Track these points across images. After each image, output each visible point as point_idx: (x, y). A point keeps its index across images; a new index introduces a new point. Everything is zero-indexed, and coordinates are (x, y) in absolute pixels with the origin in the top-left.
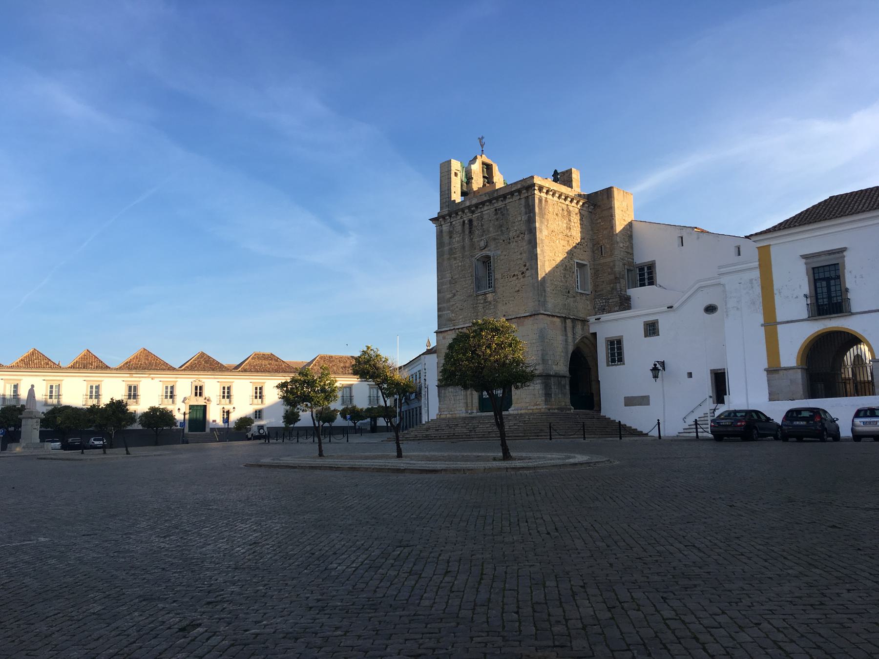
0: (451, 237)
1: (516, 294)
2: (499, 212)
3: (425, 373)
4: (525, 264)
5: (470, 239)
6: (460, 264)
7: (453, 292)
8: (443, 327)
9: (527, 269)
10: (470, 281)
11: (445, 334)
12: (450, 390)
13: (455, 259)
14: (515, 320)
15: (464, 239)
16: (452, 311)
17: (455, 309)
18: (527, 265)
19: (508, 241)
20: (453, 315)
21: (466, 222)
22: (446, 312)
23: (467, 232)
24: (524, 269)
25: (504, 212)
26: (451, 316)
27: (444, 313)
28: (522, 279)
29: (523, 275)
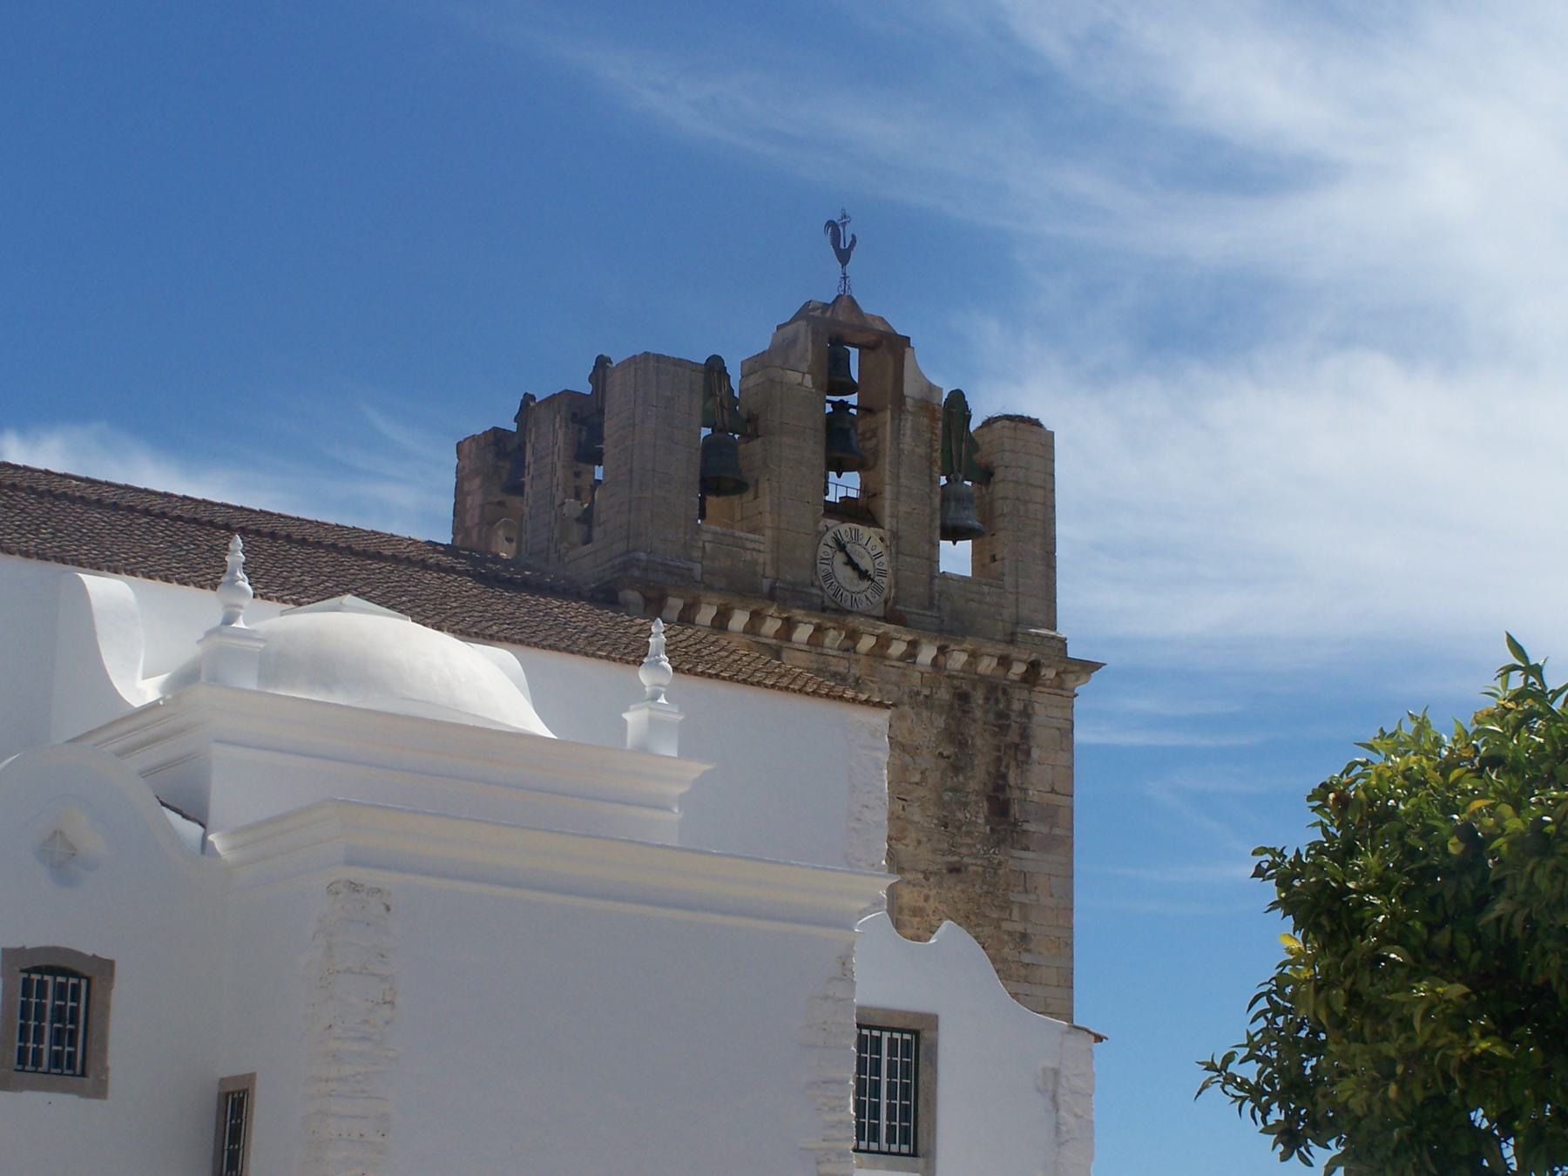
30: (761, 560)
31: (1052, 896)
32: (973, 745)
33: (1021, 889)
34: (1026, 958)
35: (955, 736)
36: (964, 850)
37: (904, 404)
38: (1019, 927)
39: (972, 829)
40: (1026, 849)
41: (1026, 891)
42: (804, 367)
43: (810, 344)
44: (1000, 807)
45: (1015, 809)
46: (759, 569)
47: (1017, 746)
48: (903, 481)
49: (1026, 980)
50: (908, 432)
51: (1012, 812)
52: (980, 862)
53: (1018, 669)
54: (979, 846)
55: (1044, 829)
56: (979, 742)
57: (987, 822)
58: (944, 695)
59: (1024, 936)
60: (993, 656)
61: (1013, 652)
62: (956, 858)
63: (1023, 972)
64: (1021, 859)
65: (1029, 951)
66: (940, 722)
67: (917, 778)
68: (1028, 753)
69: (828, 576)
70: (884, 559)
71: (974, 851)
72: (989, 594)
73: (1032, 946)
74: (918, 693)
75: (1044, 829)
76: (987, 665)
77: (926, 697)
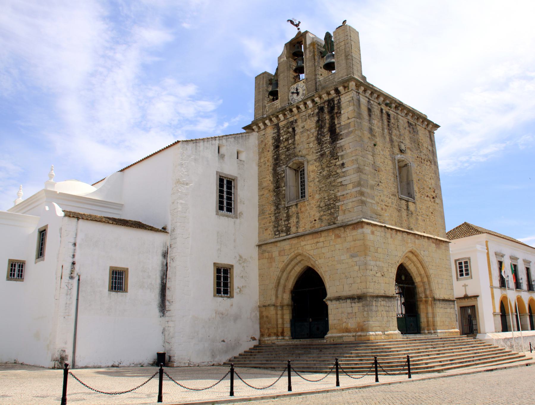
0: (370, 115)
2: (411, 126)
5: (389, 133)
7: (377, 180)
8: (368, 217)
10: (393, 179)
11: (374, 229)
12: (383, 303)
15: (383, 130)
18: (436, 192)
19: (420, 159)
21: (384, 111)
23: (386, 123)
24: (434, 196)
25: (415, 130)
26: (376, 208)
30: (278, 105)
31: (350, 148)
32: (325, 119)
33: (341, 151)
34: (344, 170)
36: (325, 148)
37: (306, 47)
38: (341, 162)
39: (326, 141)
40: (342, 139)
41: (342, 151)
42: (285, 56)
43: (286, 50)
45: (338, 130)
46: (277, 108)
47: (337, 113)
48: (308, 65)
49: (344, 176)
50: (308, 53)
51: (337, 131)
52: (329, 149)
54: (329, 145)
55: (346, 131)
56: (326, 118)
57: (330, 137)
59: (343, 164)
60: (324, 94)
61: (329, 90)
62: (323, 151)
63: (343, 174)
64: (340, 143)
65: (344, 168)
66: (316, 119)
67: (312, 136)
68: (340, 113)
69: (292, 99)
70: (304, 87)
71: (327, 147)
72: (331, 77)
73: (345, 166)
74: (310, 114)
75: (346, 131)
77: (313, 114)
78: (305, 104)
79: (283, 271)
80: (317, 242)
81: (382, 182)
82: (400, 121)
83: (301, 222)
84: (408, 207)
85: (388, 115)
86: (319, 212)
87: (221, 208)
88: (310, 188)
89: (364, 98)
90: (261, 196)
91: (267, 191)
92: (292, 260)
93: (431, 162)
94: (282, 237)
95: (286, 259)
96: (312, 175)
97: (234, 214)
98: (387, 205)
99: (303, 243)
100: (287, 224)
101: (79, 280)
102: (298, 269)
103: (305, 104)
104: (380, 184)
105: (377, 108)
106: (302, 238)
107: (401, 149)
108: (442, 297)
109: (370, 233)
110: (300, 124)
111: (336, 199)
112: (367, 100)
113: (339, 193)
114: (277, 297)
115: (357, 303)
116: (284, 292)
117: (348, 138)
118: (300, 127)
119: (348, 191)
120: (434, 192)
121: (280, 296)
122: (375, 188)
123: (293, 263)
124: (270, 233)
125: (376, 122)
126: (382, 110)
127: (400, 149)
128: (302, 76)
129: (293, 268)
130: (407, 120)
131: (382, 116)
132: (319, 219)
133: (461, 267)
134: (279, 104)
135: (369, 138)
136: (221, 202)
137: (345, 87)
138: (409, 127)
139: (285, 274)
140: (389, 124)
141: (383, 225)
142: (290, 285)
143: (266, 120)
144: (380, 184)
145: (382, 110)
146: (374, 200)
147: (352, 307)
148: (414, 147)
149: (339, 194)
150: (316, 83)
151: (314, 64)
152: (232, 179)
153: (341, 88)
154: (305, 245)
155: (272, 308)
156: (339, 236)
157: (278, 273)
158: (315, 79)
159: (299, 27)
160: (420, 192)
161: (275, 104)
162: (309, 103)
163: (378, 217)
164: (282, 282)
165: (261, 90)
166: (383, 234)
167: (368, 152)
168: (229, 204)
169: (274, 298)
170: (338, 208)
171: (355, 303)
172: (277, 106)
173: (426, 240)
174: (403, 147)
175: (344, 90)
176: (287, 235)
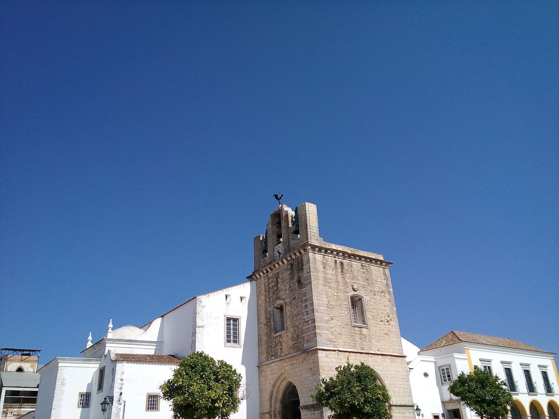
1: (385, 335)
3: (122, 384)
4: (388, 315)
6: (335, 294)
7: (331, 315)
9: (391, 320)
10: (346, 312)
11: (328, 352)
13: (330, 287)
14: (390, 357)
16: (332, 333)
17: (334, 331)
19: (374, 292)
20: (333, 337)
21: (338, 262)
22: (325, 332)
23: (339, 270)
24: (389, 319)
26: (330, 337)
27: (322, 332)
28: (388, 326)
29: (388, 323)
35: (292, 274)
44: (299, 282)
45: (302, 281)
48: (284, 231)
53: (298, 254)
58: (290, 266)
66: (289, 272)
76: (293, 257)
78: (282, 261)
79: (274, 386)
80: (293, 364)
81: (336, 316)
82: (354, 266)
83: (283, 348)
84: (361, 332)
85: (342, 264)
86: (293, 340)
87: (229, 341)
88: (288, 323)
89: (320, 255)
90: (259, 328)
91: (263, 325)
92: (279, 378)
93: (385, 293)
94: (272, 359)
95: (275, 377)
96: (288, 313)
97: (239, 345)
98: (341, 333)
99: (284, 365)
100: (275, 350)
101: (125, 405)
102: (284, 384)
103: (282, 261)
104: (334, 318)
105: (331, 260)
106: (284, 361)
107: (353, 287)
108: (399, 403)
109: (324, 356)
110: (281, 276)
111: (303, 332)
112: (322, 256)
113: (304, 327)
114: (271, 406)
115: (317, 411)
116: (276, 402)
117: (308, 287)
118: (281, 277)
119: (309, 326)
120: (389, 316)
121: (273, 406)
122: (329, 322)
123: (280, 380)
124: (265, 356)
125: (330, 272)
126: (336, 261)
127: (353, 288)
128: (281, 240)
129: (281, 384)
130: (360, 264)
131: (336, 266)
132: (294, 347)
133: (444, 373)
134: (268, 260)
135: (324, 285)
136: (228, 336)
137: (305, 250)
138: (363, 269)
139: (275, 390)
140: (342, 271)
141: (336, 349)
142: (280, 396)
143: (260, 272)
144: (334, 318)
145: (336, 261)
146: (329, 331)
147: (314, 414)
148: (367, 284)
149: (304, 328)
150: (289, 244)
151: (288, 231)
152: (237, 319)
153: (302, 251)
154: (286, 366)
155: (268, 415)
156: (305, 359)
157: (270, 388)
158: (289, 242)
159: (280, 201)
160: (374, 318)
161: (266, 259)
162: (285, 261)
163: (333, 343)
164: (274, 394)
165: (258, 248)
166: (336, 356)
167: (322, 296)
168: (235, 337)
169: (268, 407)
170: (304, 338)
171: (316, 410)
172: (267, 262)
173: (380, 356)
174: (355, 286)
175: (304, 252)
176: (275, 358)
